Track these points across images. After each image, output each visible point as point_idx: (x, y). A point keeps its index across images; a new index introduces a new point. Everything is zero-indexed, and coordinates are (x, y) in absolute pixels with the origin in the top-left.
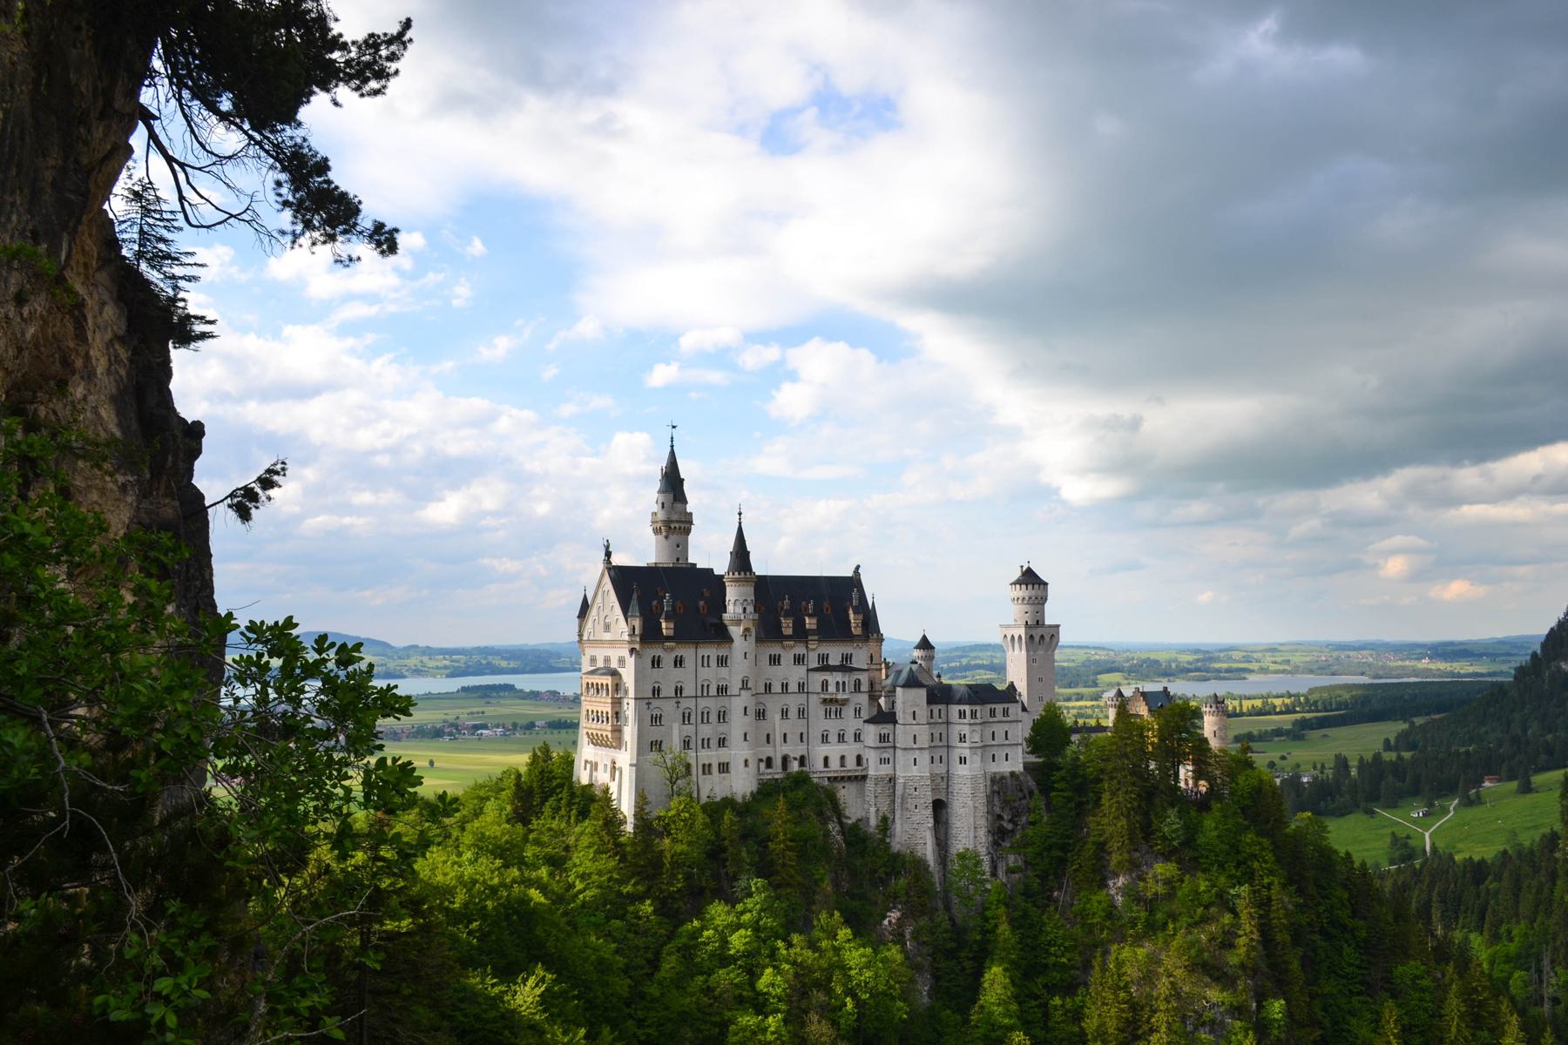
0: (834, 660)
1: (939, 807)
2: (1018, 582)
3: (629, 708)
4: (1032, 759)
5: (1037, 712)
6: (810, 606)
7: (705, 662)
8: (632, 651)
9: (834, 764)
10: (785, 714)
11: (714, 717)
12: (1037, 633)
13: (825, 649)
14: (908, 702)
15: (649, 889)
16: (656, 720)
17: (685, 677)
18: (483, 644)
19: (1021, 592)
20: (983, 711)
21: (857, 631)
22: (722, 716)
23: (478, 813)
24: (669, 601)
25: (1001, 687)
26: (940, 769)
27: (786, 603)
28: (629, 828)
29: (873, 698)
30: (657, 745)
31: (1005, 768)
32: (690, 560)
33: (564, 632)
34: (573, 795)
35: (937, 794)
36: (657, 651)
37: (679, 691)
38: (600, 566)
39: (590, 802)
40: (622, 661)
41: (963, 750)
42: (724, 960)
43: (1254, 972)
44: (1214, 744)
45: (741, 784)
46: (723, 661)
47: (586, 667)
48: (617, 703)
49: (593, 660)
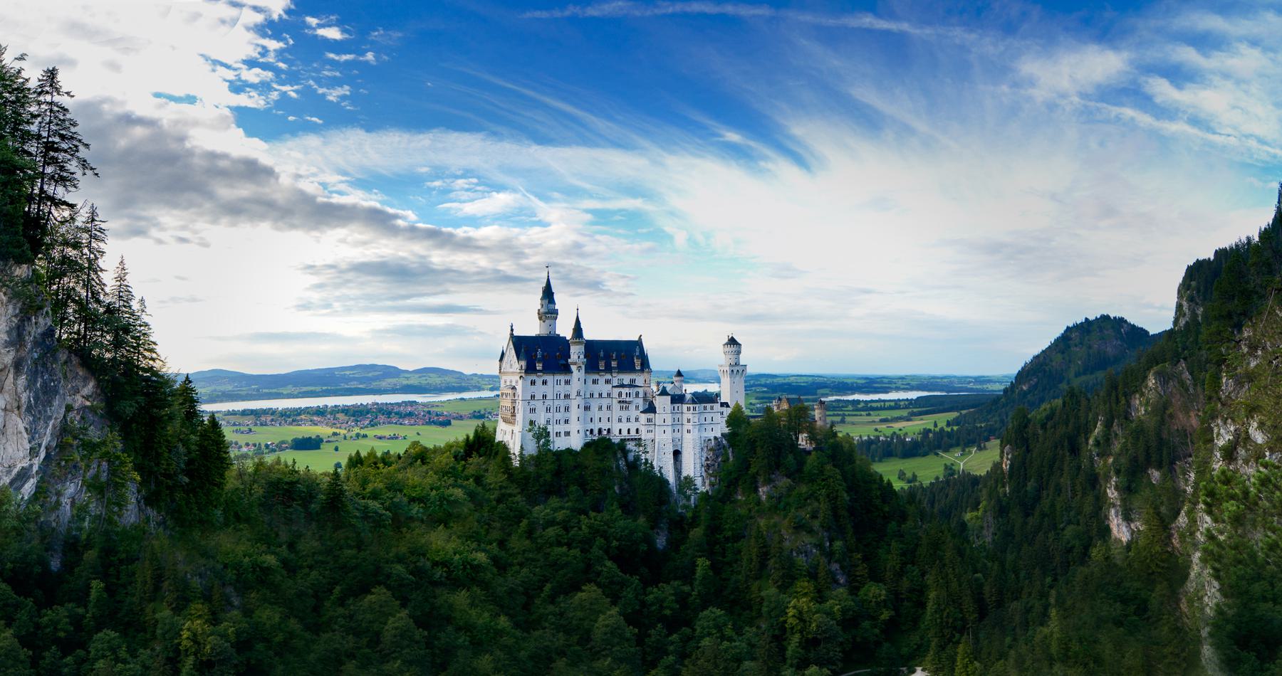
0: (626, 382)
1: (677, 454)
3: (520, 406)
4: (726, 430)
5: (732, 405)
7: (559, 382)
9: (625, 433)
10: (600, 408)
11: (562, 409)
12: (735, 369)
13: (621, 376)
14: (662, 403)
16: (533, 410)
17: (548, 389)
19: (729, 349)
20: (699, 407)
21: (638, 368)
22: (567, 409)
24: (542, 354)
26: (678, 435)
27: (602, 354)
28: (516, 463)
29: (645, 399)
30: (532, 423)
31: (711, 435)
33: (492, 368)
35: (679, 449)
36: (533, 377)
37: (545, 397)
38: (508, 336)
39: (501, 451)
41: (687, 426)
42: (551, 523)
43: (828, 529)
44: (819, 423)
45: (576, 442)
46: (567, 382)
47: (502, 385)
48: (514, 401)
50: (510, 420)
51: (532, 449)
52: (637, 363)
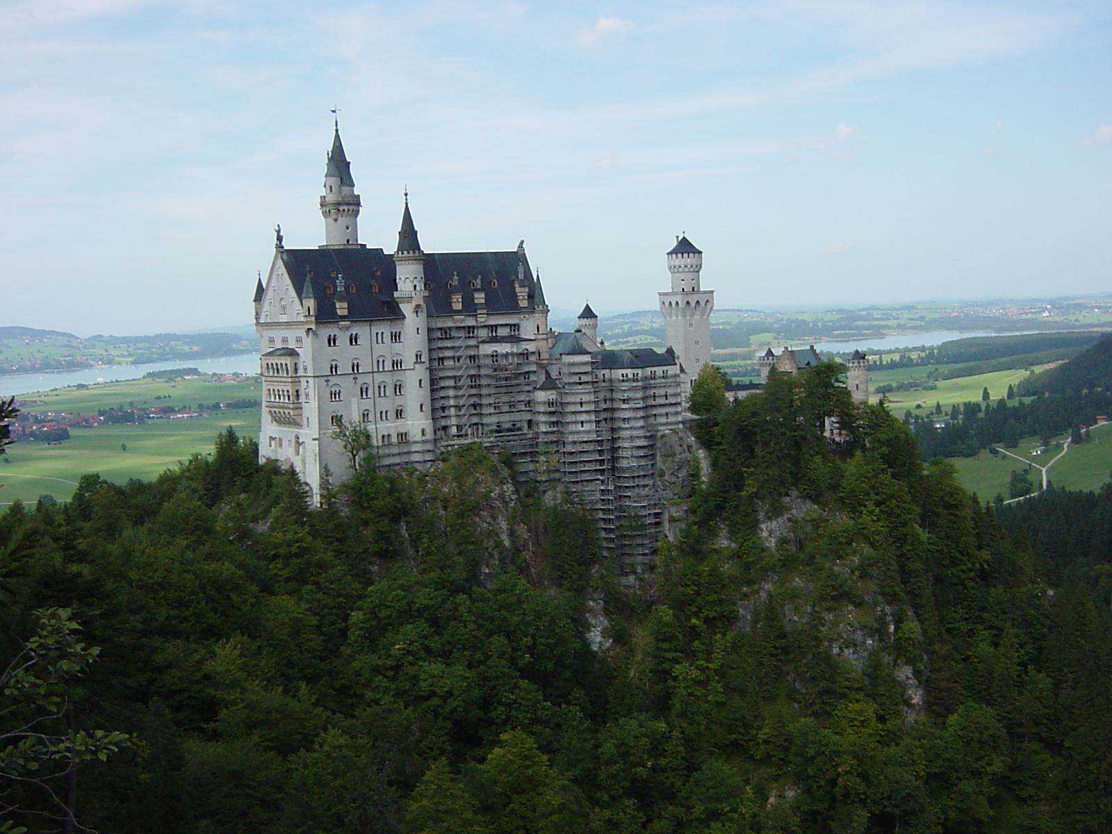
2: (674, 252)
6: (479, 281)
7: (379, 338)
8: (309, 329)
11: (390, 391)
15: (338, 552)
18: (164, 331)
19: (679, 260)
21: (524, 303)
22: (398, 388)
23: (168, 495)
24: (340, 283)
25: (661, 351)
27: (455, 281)
28: (316, 501)
30: (337, 420)
32: (359, 242)
34: (259, 469)
36: (332, 331)
37: (356, 367)
40: (299, 340)
43: (892, 599)
44: (857, 397)
48: (296, 380)
49: (272, 340)
50: (288, 419)
51: (342, 471)
52: (522, 292)
